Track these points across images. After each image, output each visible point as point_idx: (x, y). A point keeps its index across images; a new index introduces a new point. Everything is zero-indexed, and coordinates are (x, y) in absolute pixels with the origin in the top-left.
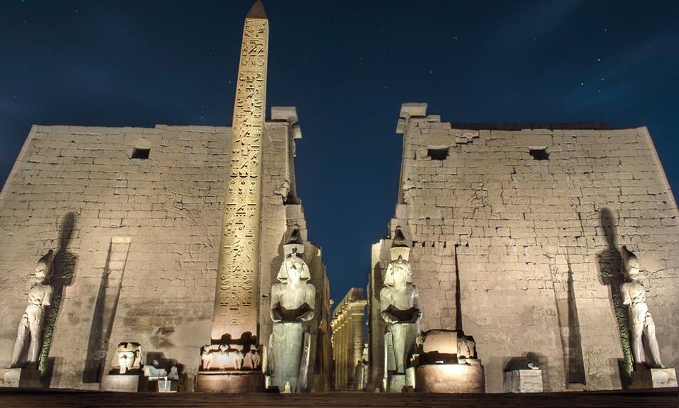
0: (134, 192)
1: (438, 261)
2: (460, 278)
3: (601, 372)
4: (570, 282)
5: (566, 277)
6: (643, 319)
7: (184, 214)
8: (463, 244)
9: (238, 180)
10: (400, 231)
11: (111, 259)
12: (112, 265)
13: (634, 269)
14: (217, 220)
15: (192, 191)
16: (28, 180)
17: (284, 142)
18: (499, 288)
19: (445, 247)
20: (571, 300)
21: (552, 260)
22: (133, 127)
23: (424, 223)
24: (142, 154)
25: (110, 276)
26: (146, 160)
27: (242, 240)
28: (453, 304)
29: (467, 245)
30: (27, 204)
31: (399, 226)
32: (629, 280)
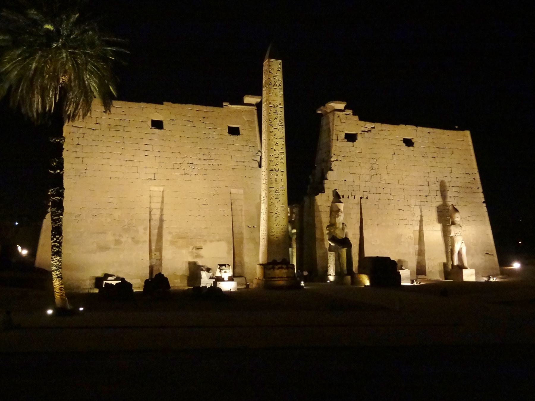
0: (158, 155)
1: (351, 207)
2: (363, 217)
3: (435, 273)
4: (421, 221)
5: (419, 218)
6: (459, 245)
7: (195, 171)
8: (365, 197)
9: (274, 173)
10: (337, 193)
11: (152, 201)
12: (153, 206)
13: (457, 218)
14: (219, 177)
15: (198, 155)
16: (76, 141)
17: (254, 122)
18: (383, 224)
19: (354, 198)
20: (421, 231)
21: (412, 209)
22: (148, 103)
23: (343, 183)
24: (158, 125)
25: (152, 213)
26: (162, 130)
27: (279, 208)
28: (358, 232)
29: (367, 198)
30: (81, 160)
31: (336, 189)
32: (453, 223)
